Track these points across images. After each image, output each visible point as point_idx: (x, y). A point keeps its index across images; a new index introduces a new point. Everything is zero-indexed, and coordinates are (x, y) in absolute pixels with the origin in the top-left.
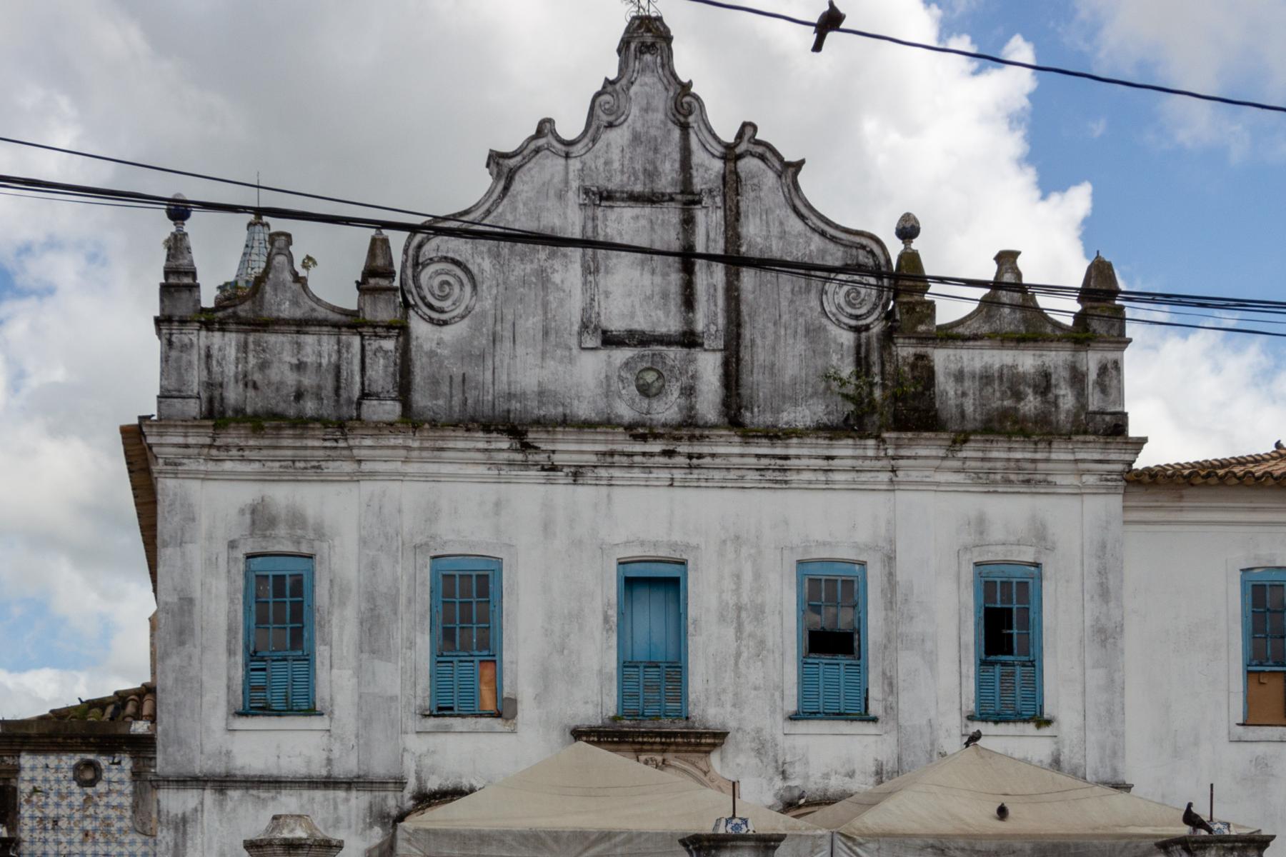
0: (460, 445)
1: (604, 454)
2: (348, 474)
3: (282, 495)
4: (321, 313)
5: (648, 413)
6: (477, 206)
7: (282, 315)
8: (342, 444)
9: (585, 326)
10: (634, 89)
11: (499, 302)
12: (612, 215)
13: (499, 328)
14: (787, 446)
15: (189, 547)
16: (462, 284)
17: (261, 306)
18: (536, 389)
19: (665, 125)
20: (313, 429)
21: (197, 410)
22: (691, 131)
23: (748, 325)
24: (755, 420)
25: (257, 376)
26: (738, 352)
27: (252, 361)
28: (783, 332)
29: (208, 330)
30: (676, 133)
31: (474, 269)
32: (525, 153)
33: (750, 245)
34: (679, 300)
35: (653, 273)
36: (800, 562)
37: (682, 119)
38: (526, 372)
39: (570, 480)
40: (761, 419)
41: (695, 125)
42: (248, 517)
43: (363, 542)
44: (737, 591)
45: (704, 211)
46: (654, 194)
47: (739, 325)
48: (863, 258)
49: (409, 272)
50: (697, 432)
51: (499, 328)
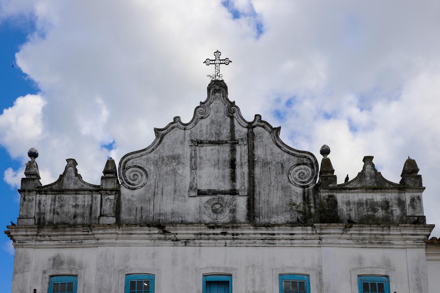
0: (138, 232)
1: (197, 234)
2: (93, 244)
3: (66, 253)
4: (86, 187)
5: (216, 219)
6: (148, 148)
7: (70, 188)
8: (90, 233)
9: (191, 188)
10: (211, 105)
11: (157, 181)
12: (203, 149)
13: (156, 190)
14: (273, 230)
15: (26, 273)
16: (142, 175)
17: (62, 185)
18: (171, 212)
19: (224, 117)
20: (78, 227)
21: (33, 222)
22: (235, 119)
23: (258, 187)
24: (261, 221)
25: (59, 210)
26: (254, 196)
27: (57, 205)
28: (272, 189)
29: (40, 194)
30: (229, 120)
31: (147, 170)
32: (168, 129)
33: (258, 158)
34: (229, 178)
35: (219, 169)
36: (280, 275)
37: (231, 115)
38: (166, 206)
39: (184, 244)
40: (263, 221)
41: (236, 117)
42: (52, 262)
43: (98, 269)
44: (253, 286)
45: (240, 146)
46: (219, 141)
47: (254, 187)
48: (305, 160)
49: (121, 171)
50: (235, 225)
51: (156, 190)
